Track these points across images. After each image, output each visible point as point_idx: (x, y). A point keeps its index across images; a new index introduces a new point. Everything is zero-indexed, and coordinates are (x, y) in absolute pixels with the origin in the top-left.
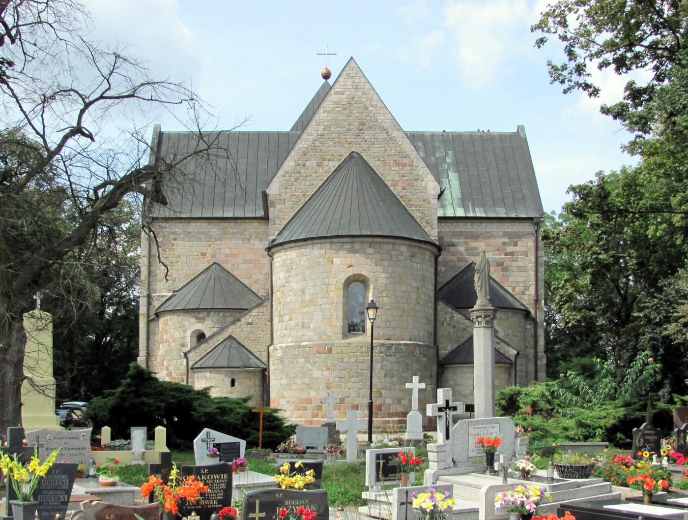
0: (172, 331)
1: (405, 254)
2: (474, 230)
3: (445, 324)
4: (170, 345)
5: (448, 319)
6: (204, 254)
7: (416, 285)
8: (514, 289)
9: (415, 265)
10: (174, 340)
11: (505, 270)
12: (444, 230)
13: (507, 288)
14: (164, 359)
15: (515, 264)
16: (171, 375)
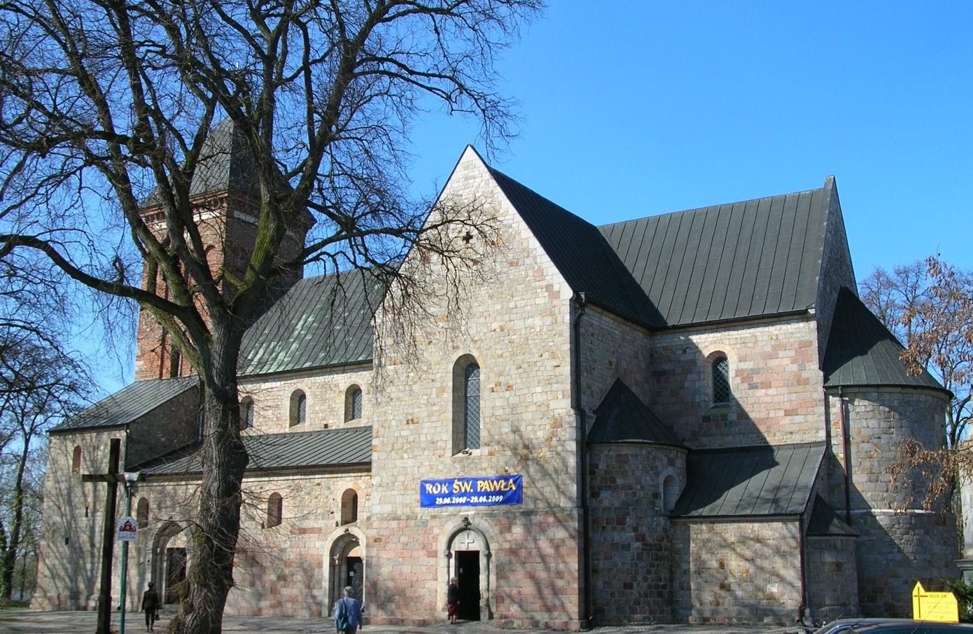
0: (638, 473)
4: (634, 494)
6: (611, 364)
10: (642, 488)
14: (628, 514)
16: (644, 540)
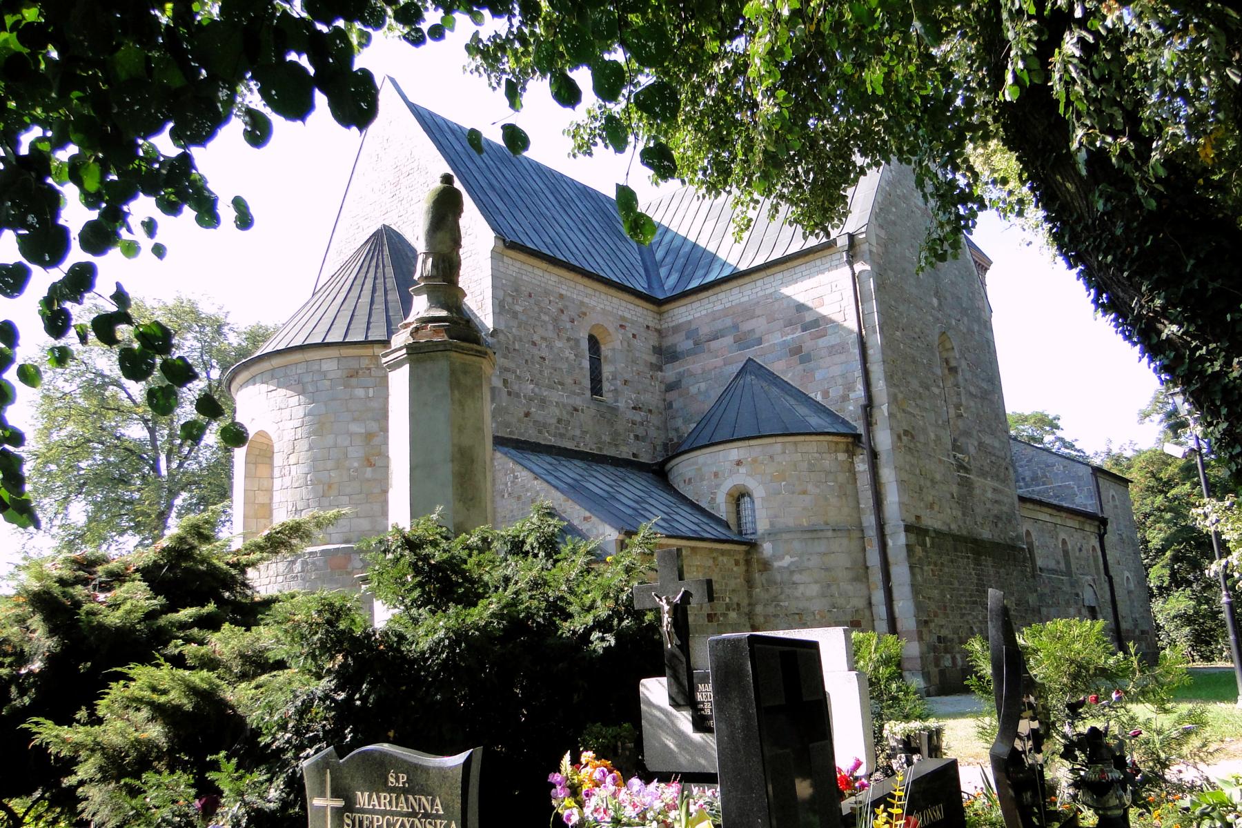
1: (331, 376)
2: (746, 299)
3: (506, 496)
5: (509, 484)
7: (363, 431)
8: (826, 394)
9: (360, 392)
11: (805, 359)
12: (699, 315)
13: (812, 395)
15: (822, 342)
